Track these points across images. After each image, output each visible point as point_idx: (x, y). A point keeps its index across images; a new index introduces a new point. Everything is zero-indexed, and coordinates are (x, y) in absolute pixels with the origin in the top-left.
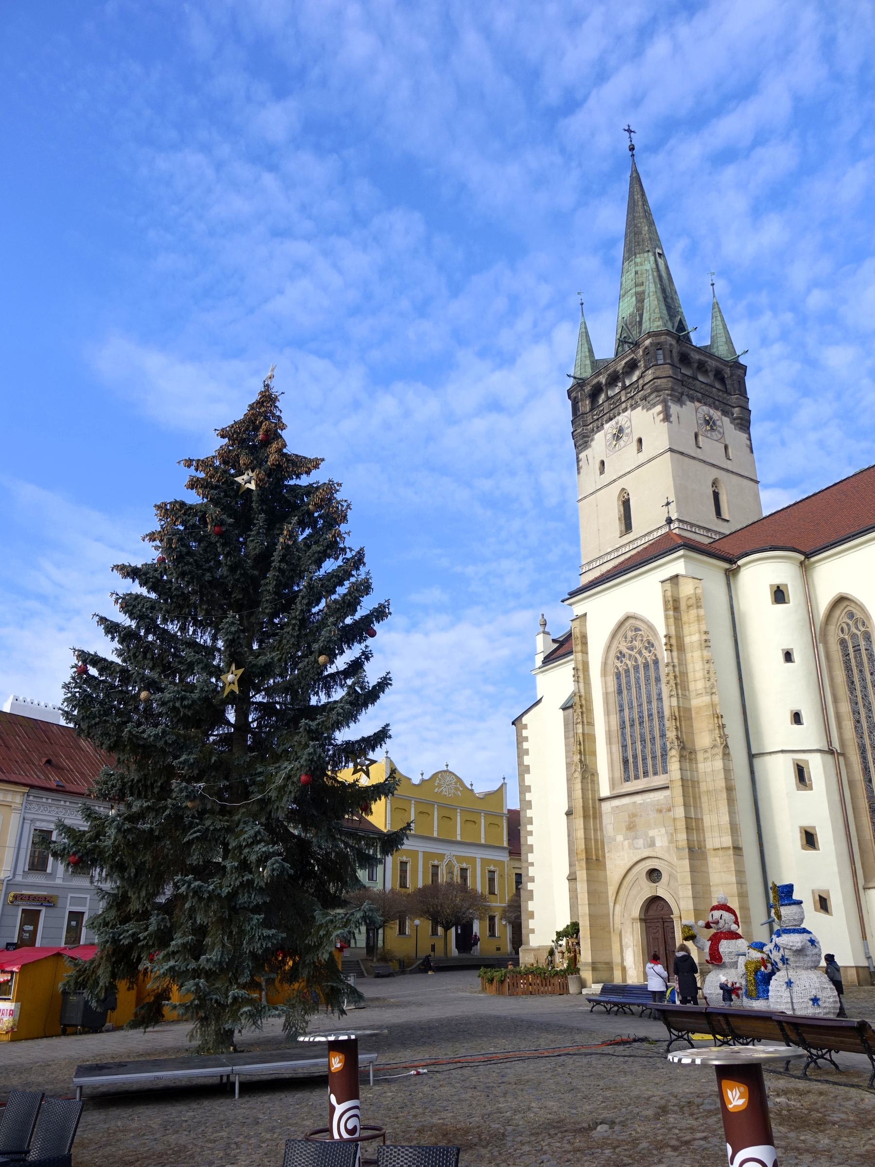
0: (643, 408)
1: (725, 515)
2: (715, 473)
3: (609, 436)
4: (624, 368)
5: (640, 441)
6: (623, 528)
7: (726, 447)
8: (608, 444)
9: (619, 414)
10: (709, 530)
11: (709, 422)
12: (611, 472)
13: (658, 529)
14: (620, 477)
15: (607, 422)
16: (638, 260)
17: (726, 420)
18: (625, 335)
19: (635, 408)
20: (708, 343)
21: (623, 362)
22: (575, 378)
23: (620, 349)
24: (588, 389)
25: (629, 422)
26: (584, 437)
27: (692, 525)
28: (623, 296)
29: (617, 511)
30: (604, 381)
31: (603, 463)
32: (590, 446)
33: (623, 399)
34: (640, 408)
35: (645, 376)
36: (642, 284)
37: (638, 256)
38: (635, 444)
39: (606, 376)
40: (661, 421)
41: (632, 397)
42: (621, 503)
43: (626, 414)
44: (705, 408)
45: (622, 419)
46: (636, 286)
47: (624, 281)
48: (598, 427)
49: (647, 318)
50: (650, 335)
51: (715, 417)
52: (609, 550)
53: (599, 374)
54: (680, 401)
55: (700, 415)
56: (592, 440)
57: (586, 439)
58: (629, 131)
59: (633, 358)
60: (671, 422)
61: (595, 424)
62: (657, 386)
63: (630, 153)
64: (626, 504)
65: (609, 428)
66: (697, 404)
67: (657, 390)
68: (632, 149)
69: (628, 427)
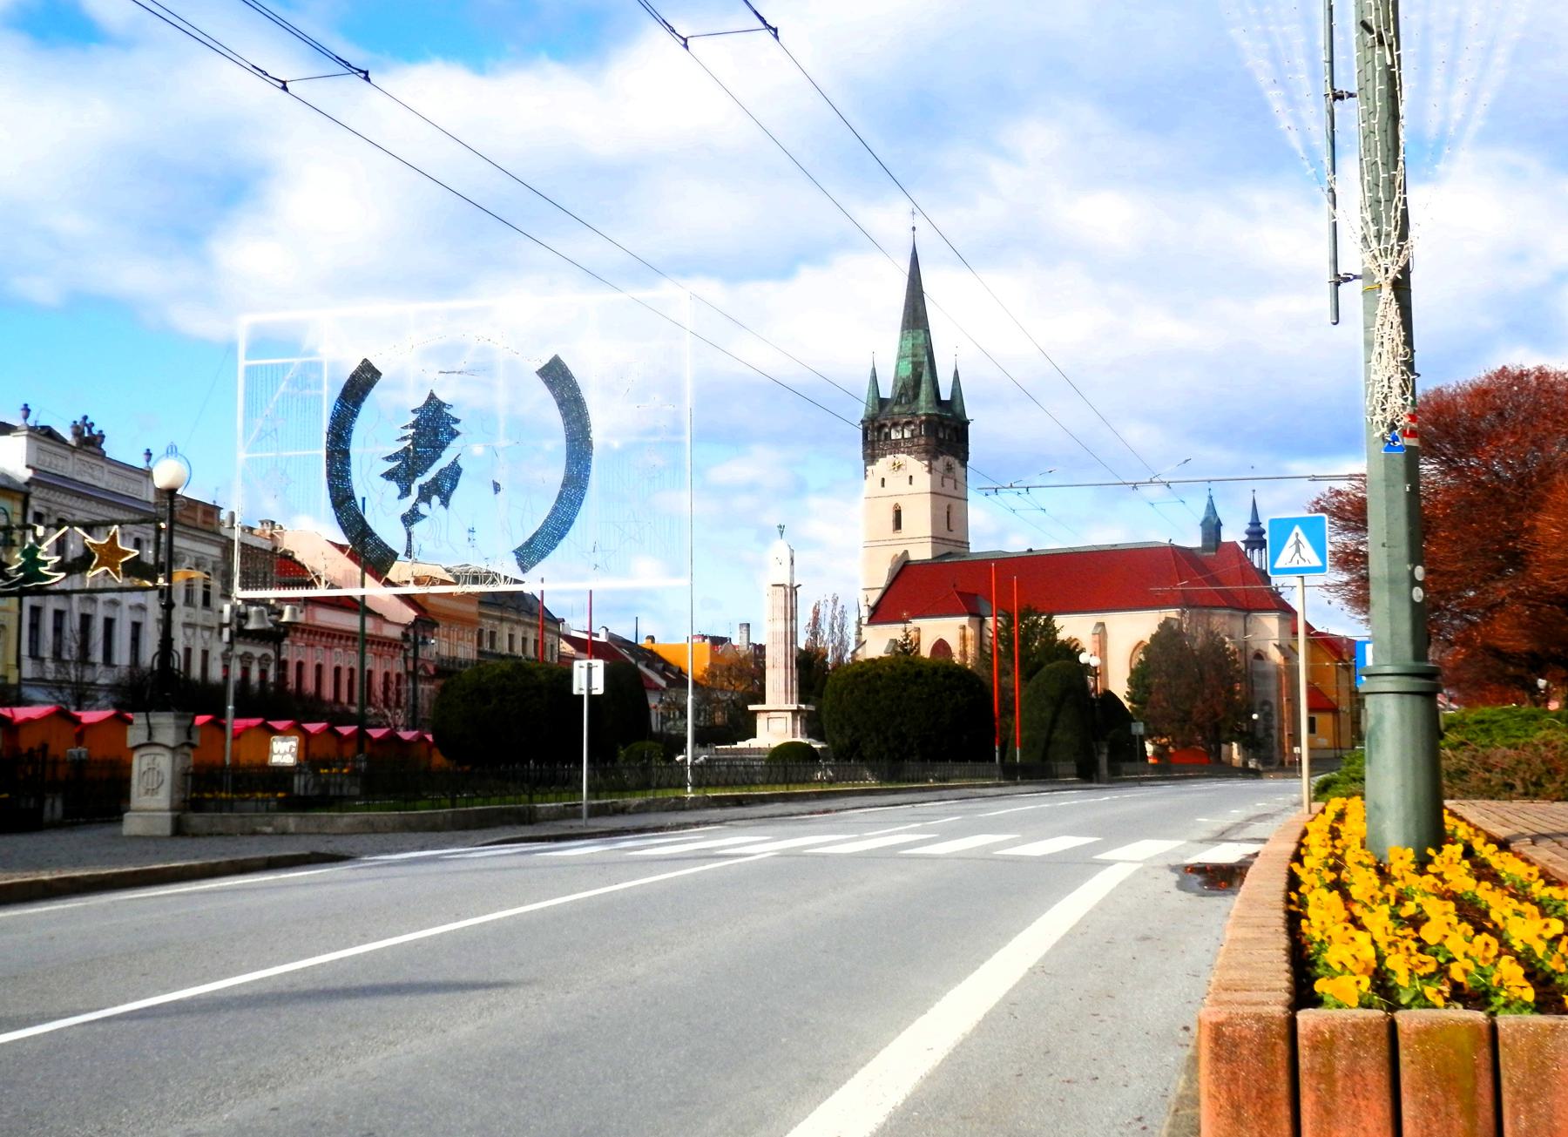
1: (951, 528)
2: (949, 500)
5: (911, 477)
10: (943, 539)
11: (949, 468)
17: (957, 461)
20: (948, 398)
24: (876, 424)
31: (883, 479)
50: (925, 414)
53: (887, 419)
54: (936, 458)
65: (890, 458)
67: (927, 452)
68: (914, 229)
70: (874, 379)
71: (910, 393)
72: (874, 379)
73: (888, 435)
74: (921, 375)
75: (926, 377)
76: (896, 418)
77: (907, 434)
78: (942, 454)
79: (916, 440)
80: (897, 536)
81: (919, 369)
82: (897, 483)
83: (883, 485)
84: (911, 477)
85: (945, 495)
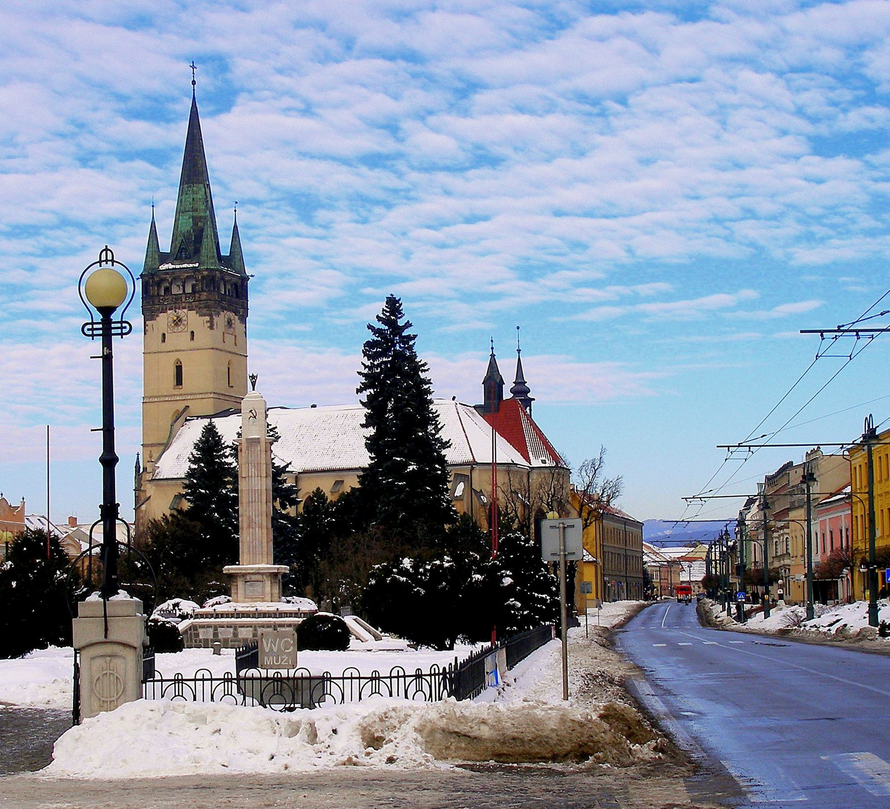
2: (230, 356)
3: (170, 320)
5: (192, 333)
7: (235, 336)
8: (169, 324)
11: (230, 323)
16: (195, 189)
25: (186, 317)
29: (173, 372)
30: (170, 280)
33: (183, 300)
34: (195, 312)
35: (200, 295)
37: (195, 185)
38: (189, 335)
44: (228, 313)
47: (184, 200)
48: (162, 309)
51: (232, 318)
55: (226, 319)
56: (158, 316)
60: (214, 329)
64: (179, 369)
66: (225, 311)
69: (185, 321)
71: (191, 248)
73: (168, 290)
74: (202, 230)
75: (208, 231)
77: (189, 290)
78: (224, 309)
79: (197, 295)
80: (177, 392)
82: (179, 339)
83: (164, 341)
84: (192, 333)
85: (226, 351)
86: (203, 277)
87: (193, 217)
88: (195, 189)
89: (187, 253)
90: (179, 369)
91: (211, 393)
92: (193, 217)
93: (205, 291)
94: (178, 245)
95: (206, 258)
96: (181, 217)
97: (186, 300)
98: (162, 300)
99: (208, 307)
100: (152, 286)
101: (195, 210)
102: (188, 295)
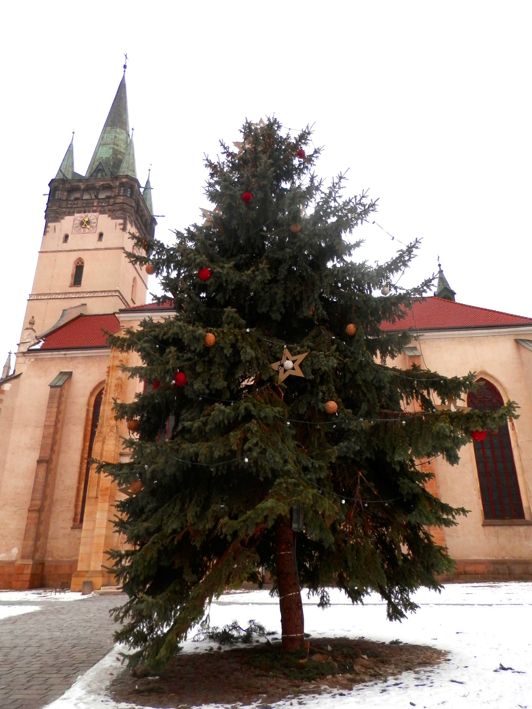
0: (109, 216)
4: (100, 186)
5: (101, 235)
6: (73, 282)
8: (75, 226)
9: (89, 212)
12: (71, 244)
13: (102, 292)
14: (79, 250)
15: (79, 212)
18: (101, 168)
19: (103, 214)
21: (101, 183)
22: (64, 175)
23: (95, 174)
24: (67, 186)
25: (95, 220)
26: (57, 214)
27: (123, 298)
28: (103, 145)
30: (83, 187)
31: (66, 237)
32: (59, 222)
33: (95, 204)
34: (106, 216)
36: (118, 145)
39: (85, 185)
40: (120, 229)
41: (103, 206)
42: (75, 266)
43: (95, 214)
45: (89, 215)
46: (114, 144)
47: (105, 137)
49: (126, 167)
50: (127, 176)
52: (58, 292)
56: (63, 218)
57: (58, 216)
58: (126, 58)
59: (109, 184)
61: (68, 210)
62: (124, 208)
63: (124, 69)
64: (79, 269)
65: (79, 217)
68: (125, 67)
69: (94, 223)
70: (70, 152)
72: (70, 152)
76: (91, 183)
79: (112, 201)
81: (119, 156)
86: (122, 185)
87: (113, 149)
88: (118, 131)
89: (104, 173)
90: (79, 269)
91: (115, 291)
92: (113, 149)
93: (122, 196)
94: (95, 168)
95: (126, 170)
96: (100, 149)
97: (98, 204)
98: (71, 204)
99: (124, 210)
100: (62, 190)
101: (118, 145)
102: (101, 201)
